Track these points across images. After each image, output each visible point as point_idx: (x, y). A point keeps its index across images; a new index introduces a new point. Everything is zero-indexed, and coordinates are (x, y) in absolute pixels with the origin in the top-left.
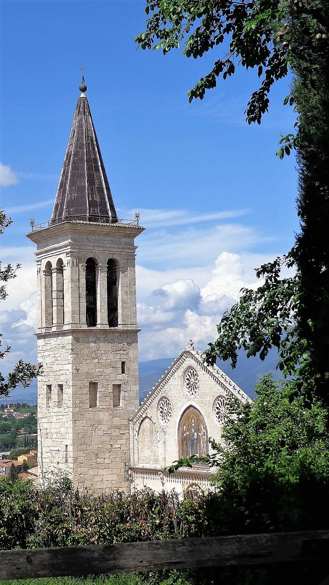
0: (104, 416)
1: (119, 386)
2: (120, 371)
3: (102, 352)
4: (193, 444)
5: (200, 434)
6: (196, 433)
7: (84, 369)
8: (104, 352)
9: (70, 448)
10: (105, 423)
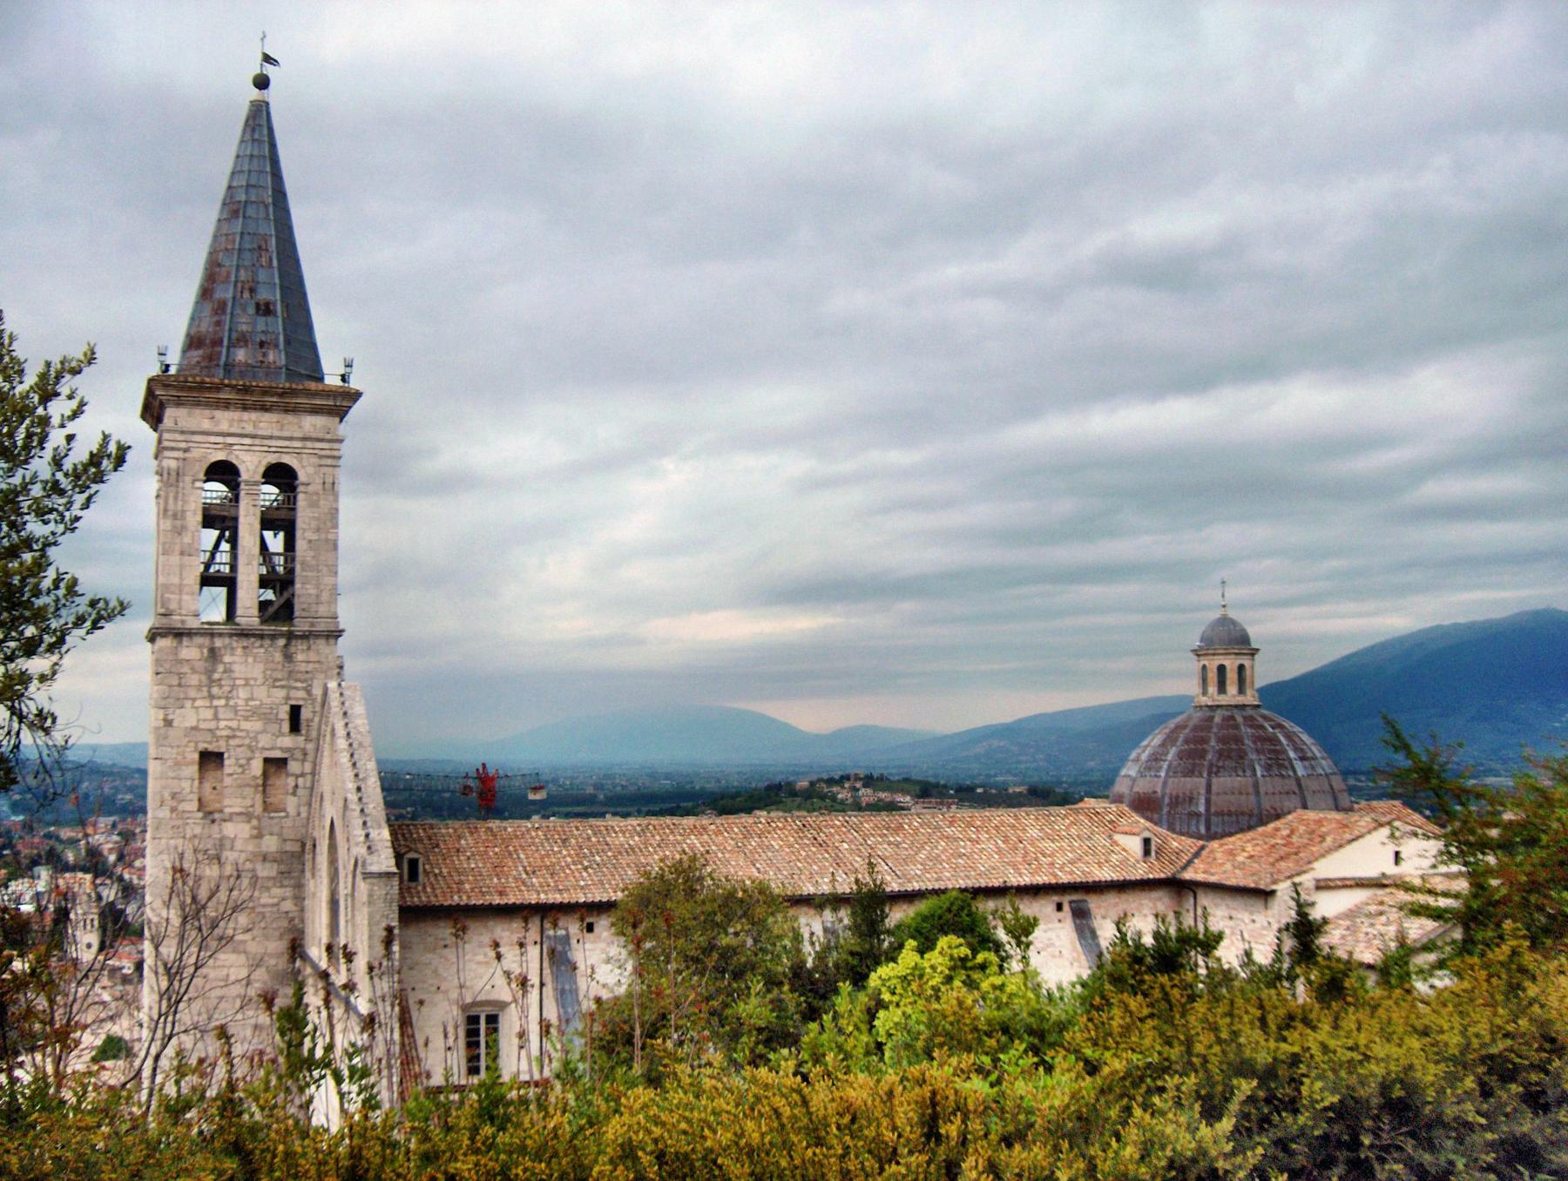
0: (237, 831)
2: (286, 726)
3: (238, 682)
7: (186, 718)
8: (242, 682)
10: (239, 845)
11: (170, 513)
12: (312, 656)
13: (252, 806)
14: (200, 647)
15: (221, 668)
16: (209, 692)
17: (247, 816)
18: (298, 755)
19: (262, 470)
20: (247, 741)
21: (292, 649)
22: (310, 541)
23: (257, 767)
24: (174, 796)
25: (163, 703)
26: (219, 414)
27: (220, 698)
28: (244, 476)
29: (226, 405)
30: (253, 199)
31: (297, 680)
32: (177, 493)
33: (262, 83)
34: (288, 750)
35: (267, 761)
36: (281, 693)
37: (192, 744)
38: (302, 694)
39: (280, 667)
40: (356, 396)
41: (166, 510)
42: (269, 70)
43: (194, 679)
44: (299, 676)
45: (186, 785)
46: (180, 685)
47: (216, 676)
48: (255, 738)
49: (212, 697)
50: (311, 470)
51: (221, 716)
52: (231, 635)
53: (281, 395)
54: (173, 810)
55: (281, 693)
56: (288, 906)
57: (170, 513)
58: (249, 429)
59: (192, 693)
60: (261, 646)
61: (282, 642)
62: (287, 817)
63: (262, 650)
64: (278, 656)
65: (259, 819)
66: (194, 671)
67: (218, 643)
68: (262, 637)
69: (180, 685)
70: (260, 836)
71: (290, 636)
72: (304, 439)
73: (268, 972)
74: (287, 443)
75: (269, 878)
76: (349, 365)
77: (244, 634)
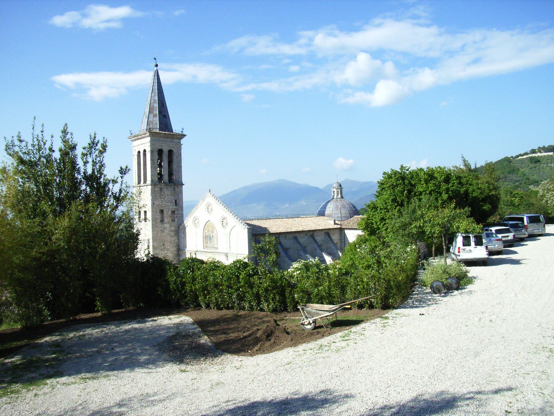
0: (167, 225)
1: (174, 211)
4: (210, 239)
5: (214, 234)
6: (212, 234)
9: (151, 241)
12: (178, 189)
17: (169, 223)
18: (177, 210)
19: (168, 151)
23: (170, 212)
24: (155, 219)
34: (175, 209)
36: (173, 197)
38: (177, 197)
45: (157, 216)
49: (161, 198)
56: (176, 241)
59: (158, 198)
64: (173, 190)
65: (171, 223)
66: (158, 193)
70: (171, 227)
76: (183, 129)
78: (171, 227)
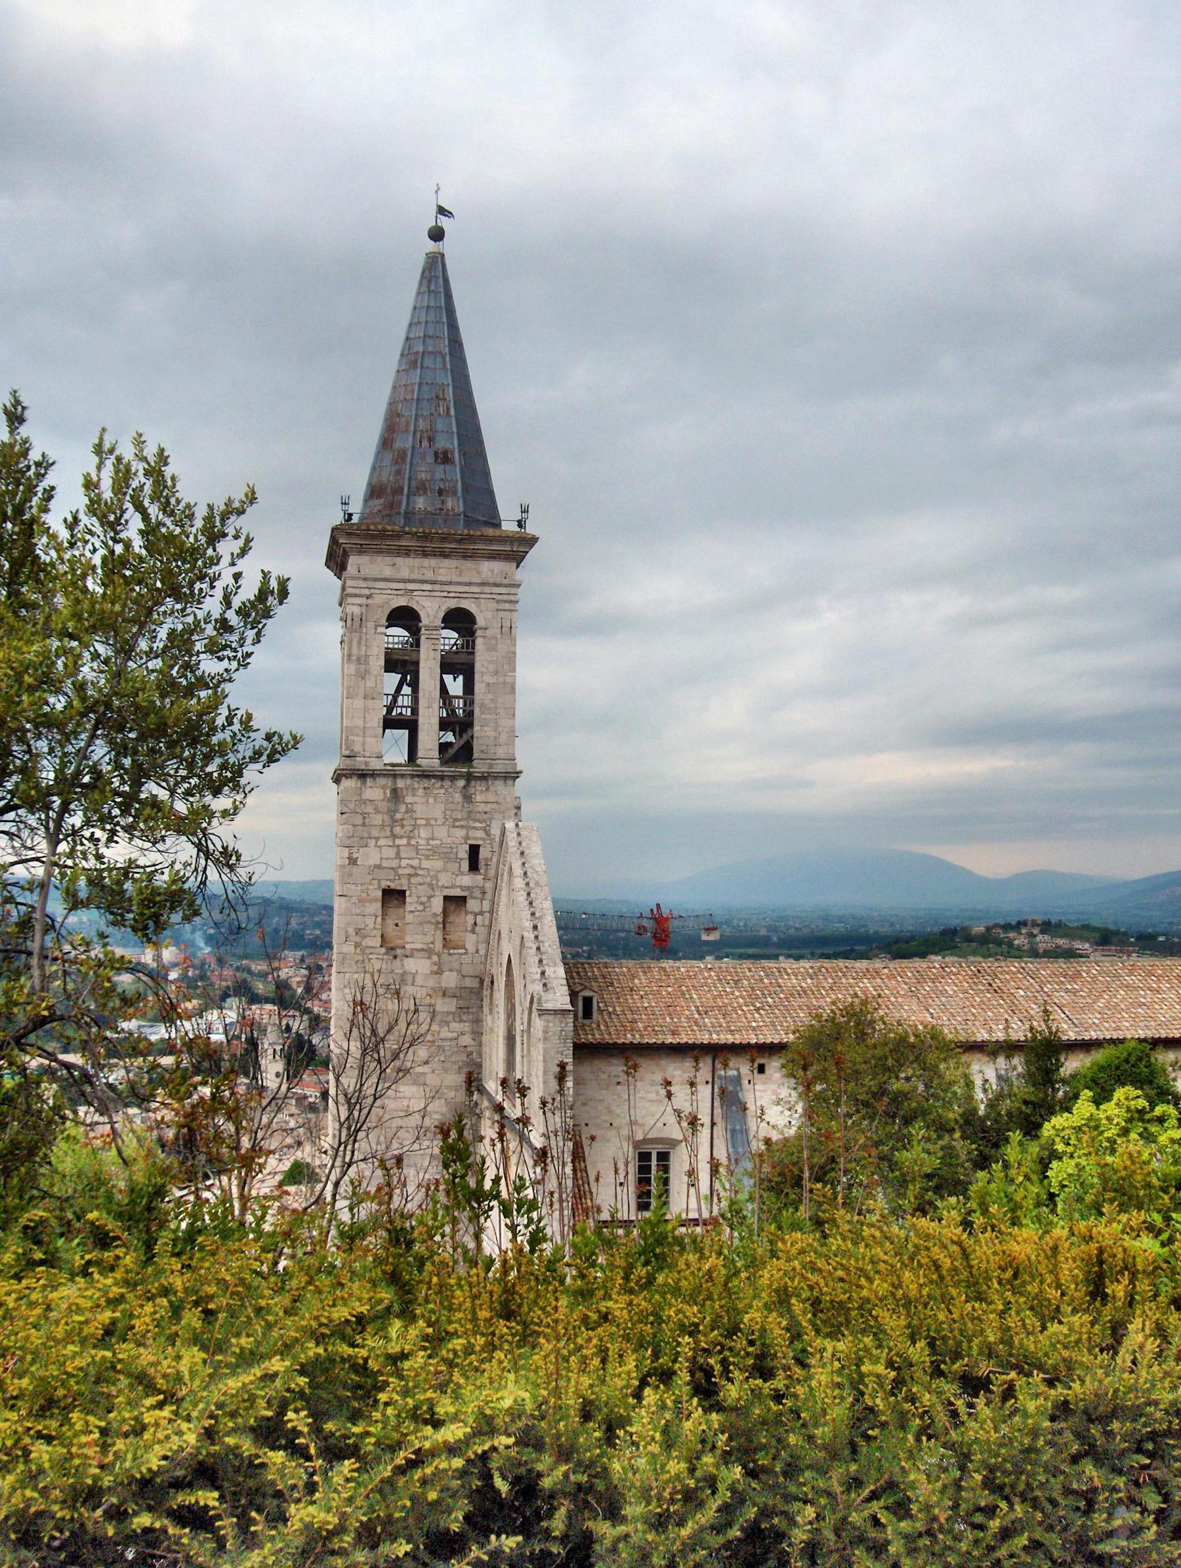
0: (419, 966)
1: (463, 899)
2: (465, 865)
3: (419, 822)
7: (370, 856)
8: (424, 822)
10: (419, 980)
11: (354, 658)
12: (491, 797)
13: (432, 943)
14: (384, 787)
15: (403, 808)
16: (392, 831)
17: (429, 952)
18: (477, 893)
19: (442, 615)
20: (428, 880)
21: (472, 791)
22: (488, 684)
23: (437, 905)
25: (347, 843)
26: (399, 561)
27: (401, 837)
28: (425, 621)
29: (407, 552)
30: (430, 349)
31: (476, 821)
32: (361, 638)
33: (437, 234)
34: (468, 888)
35: (447, 899)
36: (461, 833)
37: (376, 882)
38: (481, 834)
39: (460, 807)
40: (532, 541)
41: (349, 656)
42: (444, 222)
43: (378, 819)
44: (478, 816)
45: (370, 921)
46: (364, 825)
47: (398, 816)
48: (436, 877)
49: (394, 836)
50: (489, 615)
51: (403, 855)
52: (413, 776)
53: (460, 541)
54: (357, 945)
55: (461, 833)
56: (466, 1040)
57: (354, 658)
58: (429, 575)
59: (375, 833)
60: (442, 787)
61: (461, 783)
62: (466, 953)
63: (443, 791)
64: (458, 797)
66: (377, 811)
67: (400, 783)
68: (442, 778)
69: (364, 825)
70: (439, 972)
71: (469, 777)
72: (483, 584)
73: (447, 1104)
74: (467, 589)
75: (448, 1013)
76: (525, 511)
77: (426, 775)
78: (439, 972)
